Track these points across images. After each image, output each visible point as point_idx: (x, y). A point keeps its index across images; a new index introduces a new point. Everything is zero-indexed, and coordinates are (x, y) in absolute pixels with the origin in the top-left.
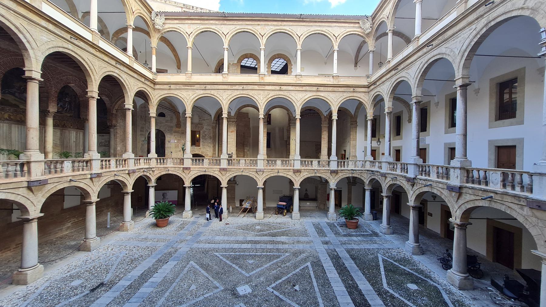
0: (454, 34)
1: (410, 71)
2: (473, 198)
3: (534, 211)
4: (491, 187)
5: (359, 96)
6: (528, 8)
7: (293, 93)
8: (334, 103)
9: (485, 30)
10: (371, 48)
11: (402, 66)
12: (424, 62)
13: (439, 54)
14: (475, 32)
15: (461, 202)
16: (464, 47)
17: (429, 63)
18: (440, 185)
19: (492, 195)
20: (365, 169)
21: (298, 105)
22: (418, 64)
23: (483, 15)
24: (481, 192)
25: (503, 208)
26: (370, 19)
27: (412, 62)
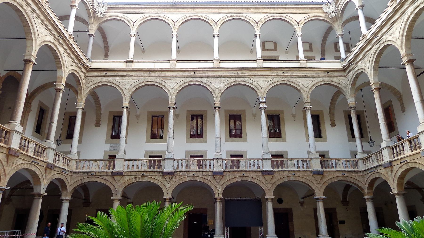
0: (214, 76)
1: (167, 81)
2: (231, 177)
3: (265, 176)
4: (241, 169)
5: (81, 76)
6: (254, 85)
7: (37, 20)
8: (66, 69)
9: (233, 84)
10: (92, 32)
11: (157, 73)
12: (185, 81)
13: (201, 82)
14: (228, 82)
15: (222, 182)
16: (222, 86)
17: (189, 83)
18: (204, 173)
19: (244, 173)
20: (71, 170)
21: (38, 43)
22: (178, 80)
23: (233, 76)
24: (237, 172)
25: (249, 179)
26: (106, 7)
27: (172, 76)
